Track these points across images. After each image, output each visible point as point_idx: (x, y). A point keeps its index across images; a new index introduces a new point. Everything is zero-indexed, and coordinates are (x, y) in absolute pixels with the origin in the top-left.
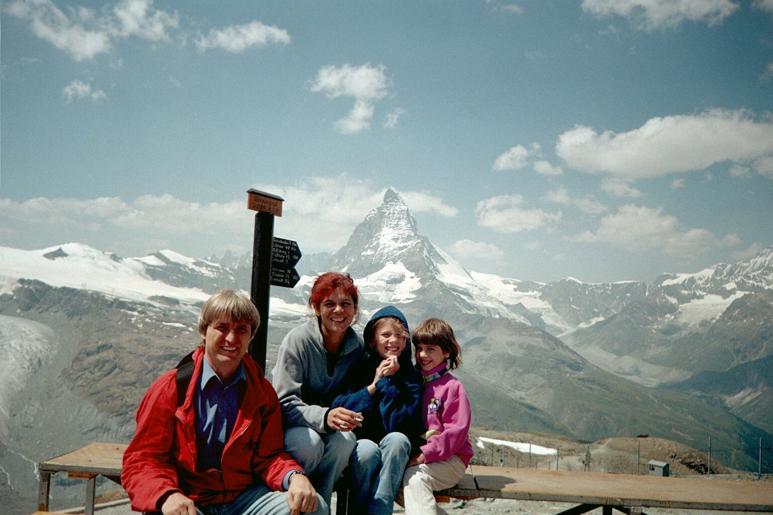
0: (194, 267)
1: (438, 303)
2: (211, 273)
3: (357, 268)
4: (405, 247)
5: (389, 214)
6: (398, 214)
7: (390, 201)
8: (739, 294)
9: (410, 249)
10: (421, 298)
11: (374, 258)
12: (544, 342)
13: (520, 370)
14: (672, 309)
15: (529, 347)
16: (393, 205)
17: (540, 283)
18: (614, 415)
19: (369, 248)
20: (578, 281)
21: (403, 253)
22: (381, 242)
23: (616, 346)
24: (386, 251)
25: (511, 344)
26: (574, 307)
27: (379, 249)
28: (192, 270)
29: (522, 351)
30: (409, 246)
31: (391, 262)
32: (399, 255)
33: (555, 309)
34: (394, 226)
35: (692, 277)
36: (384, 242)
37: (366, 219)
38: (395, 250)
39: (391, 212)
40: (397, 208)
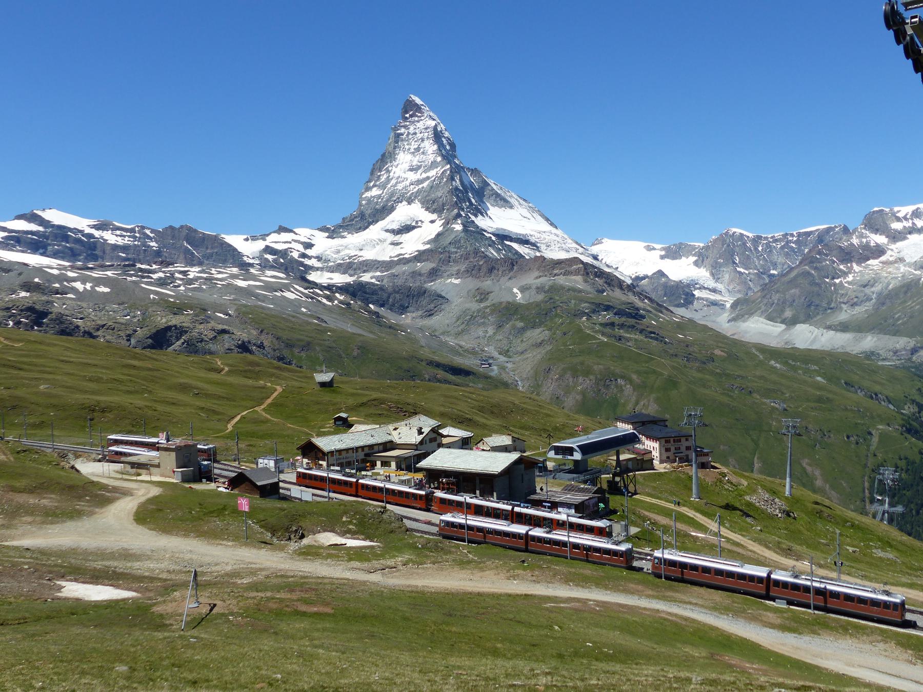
0: (93, 231)
2: (119, 239)
3: (356, 217)
4: (428, 178)
7: (411, 116)
12: (586, 281)
13: (520, 324)
14: (879, 251)
16: (413, 122)
17: (697, 244)
18: (634, 377)
19: (374, 186)
20: (745, 233)
23: (788, 314)
24: (400, 186)
26: (742, 270)
27: (389, 186)
28: (90, 236)
32: (417, 192)
33: (715, 276)
35: (918, 208)
36: (396, 175)
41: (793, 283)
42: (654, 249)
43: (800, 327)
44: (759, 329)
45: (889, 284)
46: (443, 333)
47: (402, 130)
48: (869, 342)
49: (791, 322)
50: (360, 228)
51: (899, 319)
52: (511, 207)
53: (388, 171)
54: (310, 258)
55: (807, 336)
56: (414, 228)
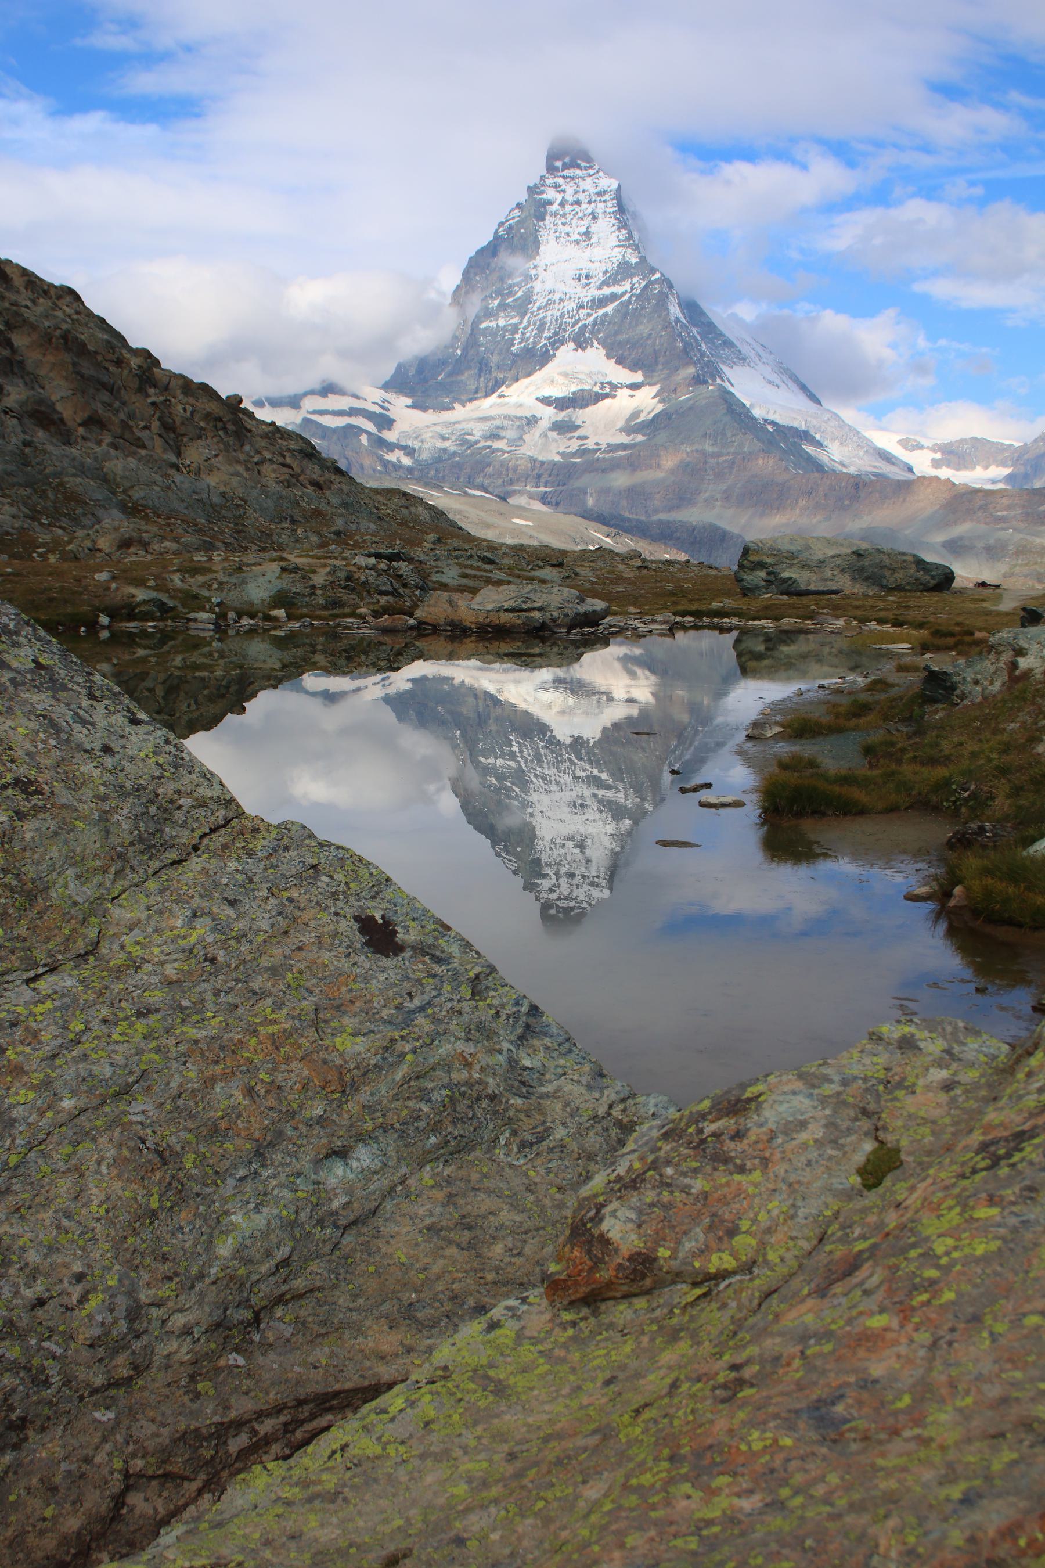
1: (716, 450)
4: (613, 297)
5: (562, 204)
6: (590, 202)
7: (566, 167)
9: (629, 301)
11: (518, 336)
16: (572, 178)
19: (503, 307)
21: (606, 315)
22: (538, 286)
30: (625, 293)
31: (572, 345)
34: (578, 237)
36: (548, 286)
37: (496, 232)
38: (583, 307)
39: (570, 198)
40: (588, 184)
50: (476, 392)
53: (529, 278)
54: (391, 447)
56: (599, 398)
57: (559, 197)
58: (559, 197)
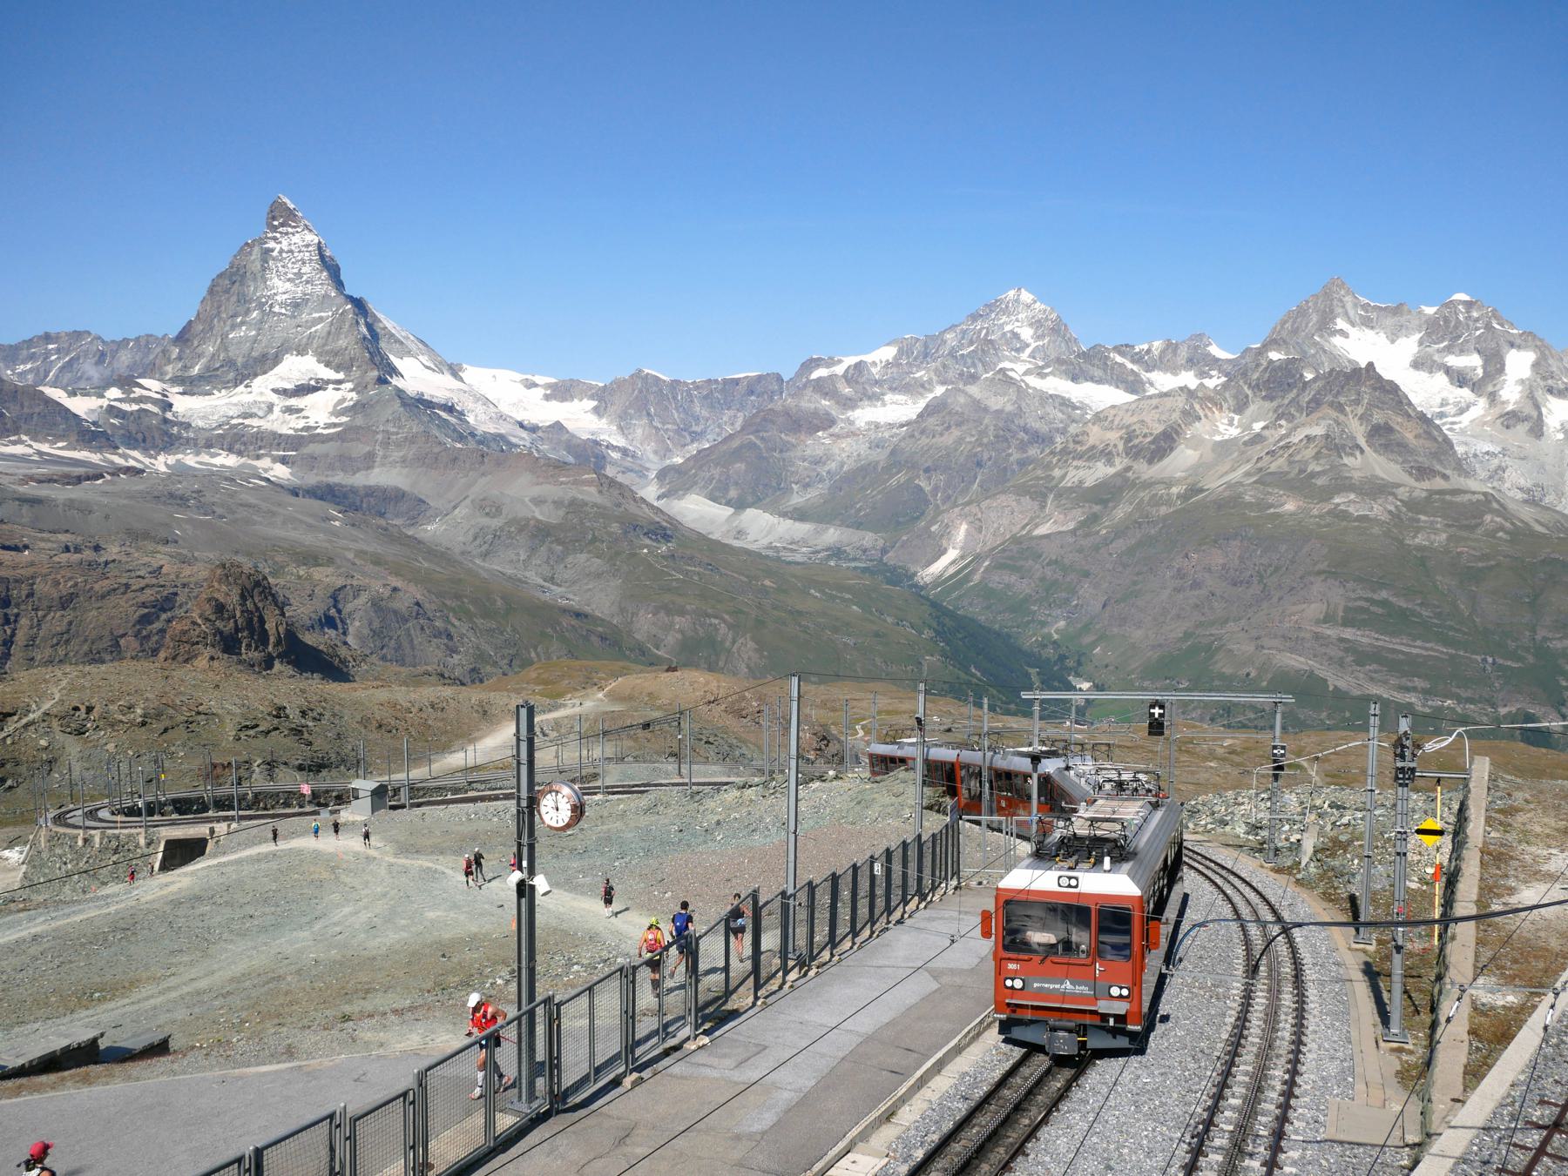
4: (321, 319)
7: (282, 225)
8: (940, 390)
10: (359, 421)
12: (600, 492)
14: (827, 422)
15: (575, 506)
25: (538, 501)
29: (561, 513)
40: (296, 239)
41: (737, 454)
42: (536, 385)
43: (750, 513)
44: (697, 510)
45: (842, 464)
46: (463, 553)
47: (271, 244)
48: (832, 535)
49: (740, 505)
51: (860, 510)
52: (409, 353)
55: (762, 528)
56: (315, 389)
57: (278, 247)
58: (278, 247)
